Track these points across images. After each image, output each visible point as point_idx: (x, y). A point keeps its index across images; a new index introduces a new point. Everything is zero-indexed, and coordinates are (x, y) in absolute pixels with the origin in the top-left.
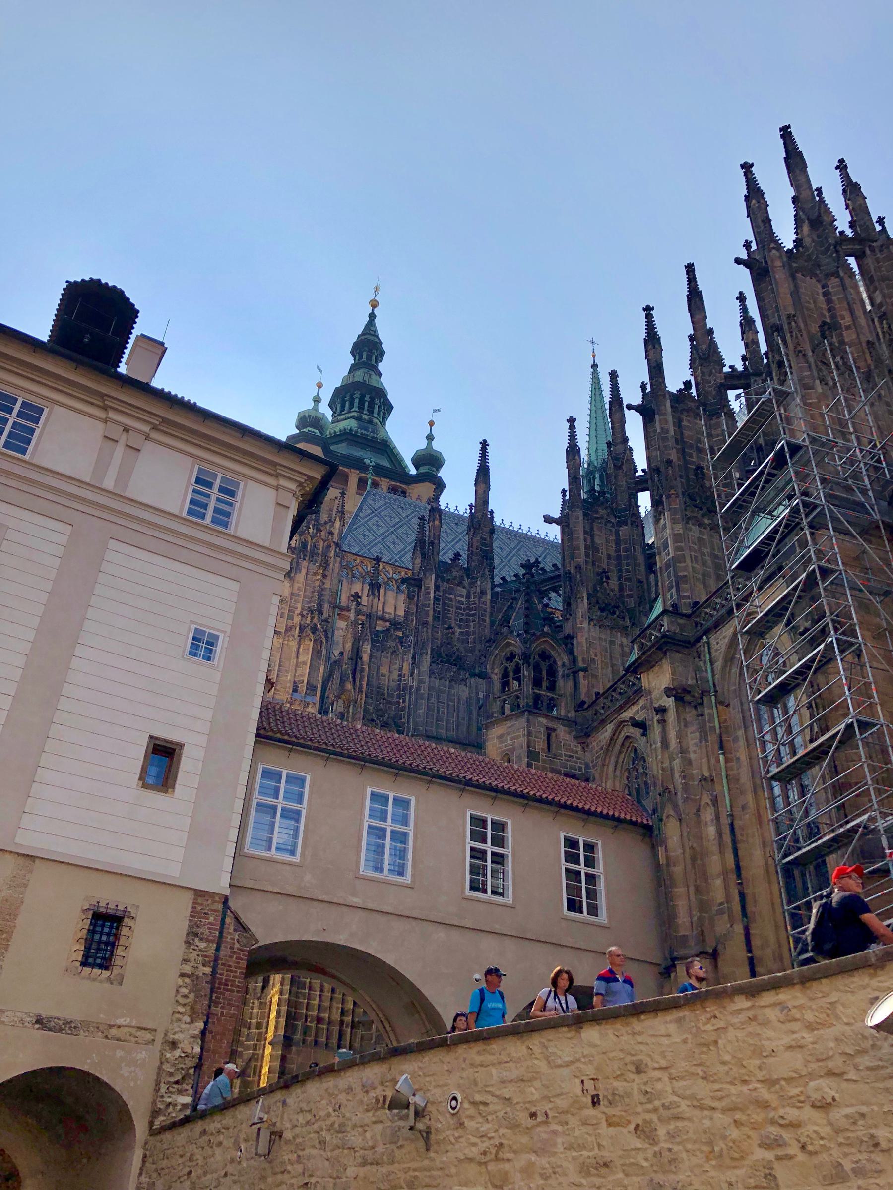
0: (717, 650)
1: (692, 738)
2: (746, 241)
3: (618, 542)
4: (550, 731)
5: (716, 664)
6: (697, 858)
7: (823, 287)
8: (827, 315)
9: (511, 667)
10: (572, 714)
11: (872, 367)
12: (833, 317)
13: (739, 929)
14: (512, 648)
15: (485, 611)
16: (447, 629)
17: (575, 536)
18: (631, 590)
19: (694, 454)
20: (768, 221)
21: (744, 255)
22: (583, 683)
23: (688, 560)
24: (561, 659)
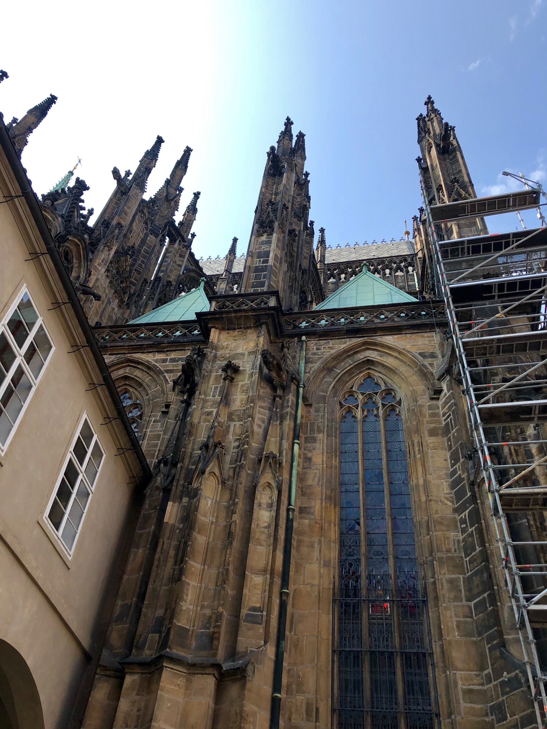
0: (315, 354)
1: (261, 414)
3: (143, 241)
5: (310, 365)
6: (238, 538)
13: (271, 651)
17: (129, 204)
18: (135, 279)
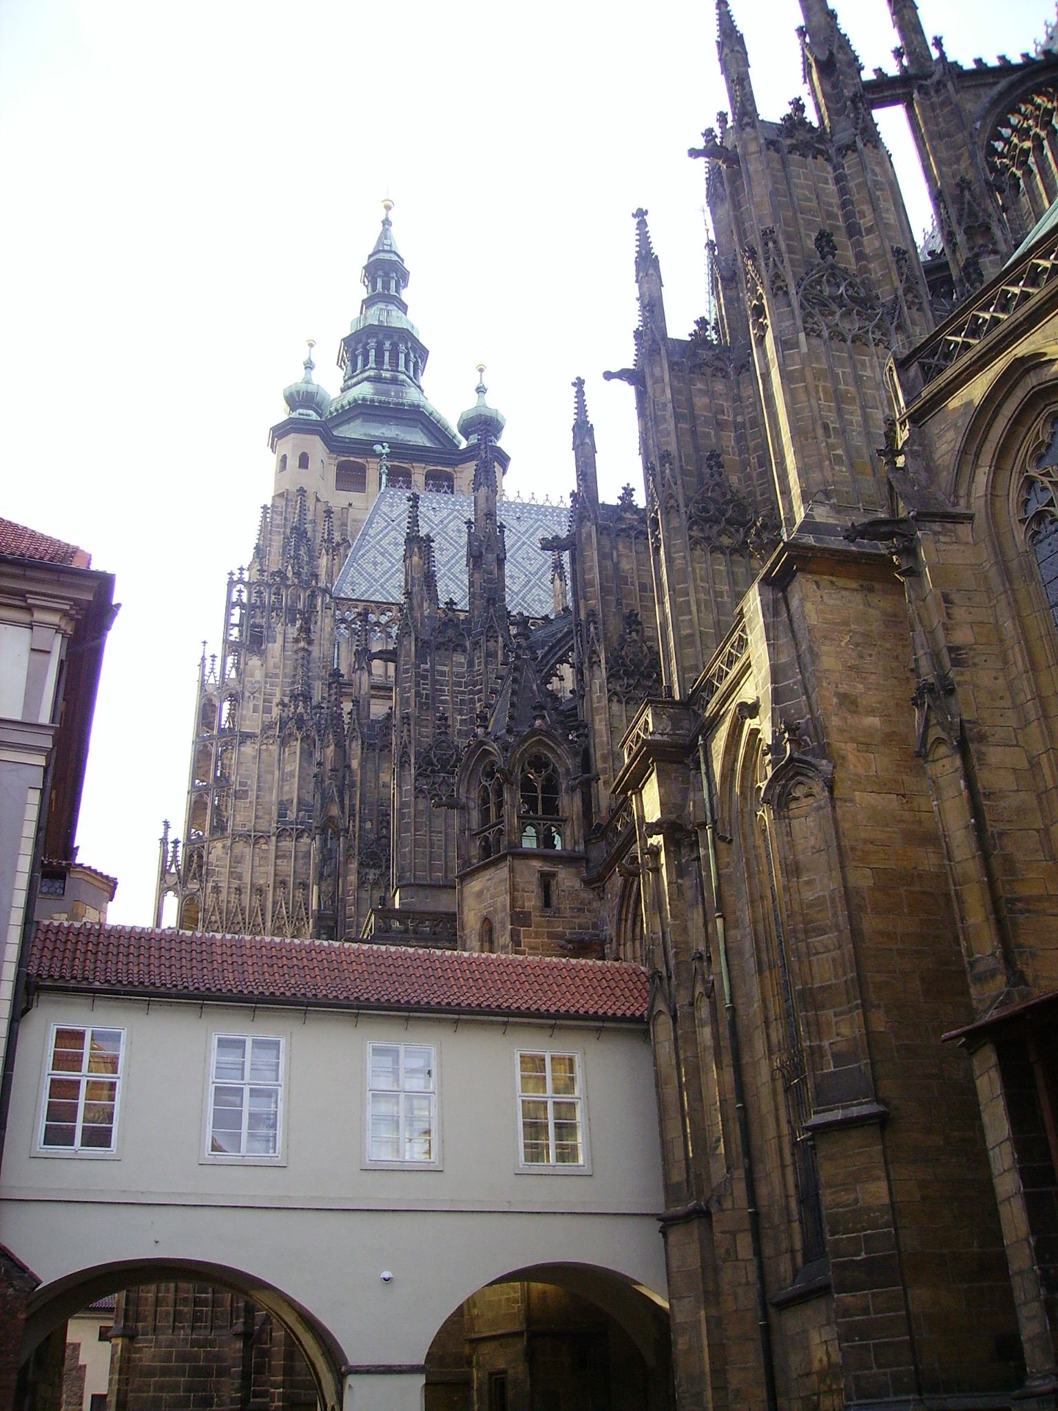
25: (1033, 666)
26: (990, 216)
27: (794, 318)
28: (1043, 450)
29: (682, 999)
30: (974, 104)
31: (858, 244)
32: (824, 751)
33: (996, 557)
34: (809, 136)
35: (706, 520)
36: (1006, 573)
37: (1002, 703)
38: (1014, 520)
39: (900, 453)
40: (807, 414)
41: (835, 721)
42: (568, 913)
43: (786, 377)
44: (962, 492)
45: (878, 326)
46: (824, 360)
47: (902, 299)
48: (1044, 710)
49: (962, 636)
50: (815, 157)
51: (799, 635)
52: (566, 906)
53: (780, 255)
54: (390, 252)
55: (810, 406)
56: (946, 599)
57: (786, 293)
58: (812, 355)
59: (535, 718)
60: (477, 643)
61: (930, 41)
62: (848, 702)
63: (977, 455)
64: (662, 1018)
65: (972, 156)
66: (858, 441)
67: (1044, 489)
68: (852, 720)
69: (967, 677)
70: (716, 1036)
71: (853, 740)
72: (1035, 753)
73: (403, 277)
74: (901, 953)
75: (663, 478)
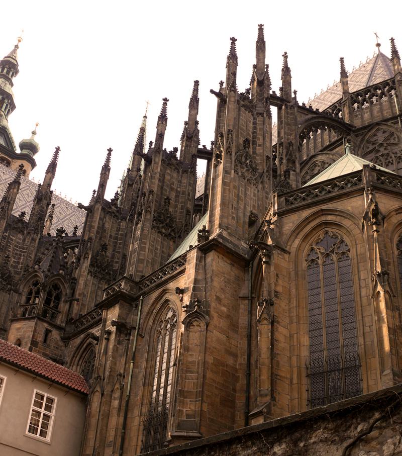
2: (221, 81)
4: (48, 332)
7: (254, 119)
8: (251, 135)
9: (34, 289)
10: (64, 325)
11: (265, 171)
12: (254, 137)
14: (38, 279)
15: (32, 251)
16: (6, 257)
19: (168, 190)
20: (235, 74)
21: (217, 90)
22: (76, 307)
23: (147, 250)
24: (66, 290)
25: (298, 306)
26: (296, 158)
27: (231, 164)
28: (320, 241)
29: (107, 390)
30: (301, 118)
31: (255, 148)
32: (208, 313)
33: (295, 268)
34: (249, 104)
35: (160, 221)
36: (297, 274)
37: (285, 314)
38: (304, 259)
39: (272, 224)
40: (227, 198)
41: (213, 304)
42: (52, 348)
43: (224, 183)
44: (289, 244)
45: (256, 179)
46: (237, 182)
47: (265, 173)
48: (299, 321)
49: (279, 289)
50: (249, 112)
51: (207, 272)
52: (52, 344)
53: (232, 141)
54: (15, 60)
55: (229, 196)
56: (277, 275)
57: (231, 154)
58: (234, 180)
59: (60, 270)
60: (29, 233)
61: (293, 90)
62: (218, 299)
63: (298, 234)
64: (97, 393)
65: (296, 136)
66: (241, 215)
67: (316, 253)
68: (218, 306)
69: (278, 302)
70: (120, 405)
71: (217, 313)
72: (292, 333)
73: (16, 72)
74: (216, 388)
75: (148, 199)
